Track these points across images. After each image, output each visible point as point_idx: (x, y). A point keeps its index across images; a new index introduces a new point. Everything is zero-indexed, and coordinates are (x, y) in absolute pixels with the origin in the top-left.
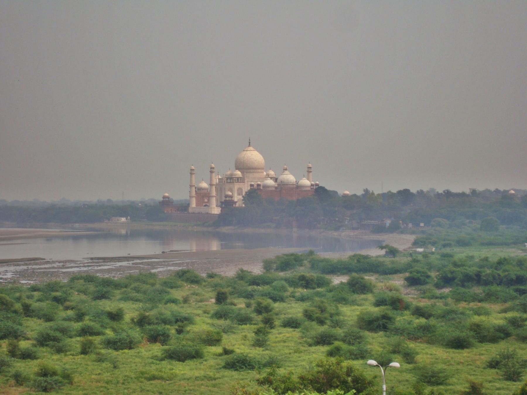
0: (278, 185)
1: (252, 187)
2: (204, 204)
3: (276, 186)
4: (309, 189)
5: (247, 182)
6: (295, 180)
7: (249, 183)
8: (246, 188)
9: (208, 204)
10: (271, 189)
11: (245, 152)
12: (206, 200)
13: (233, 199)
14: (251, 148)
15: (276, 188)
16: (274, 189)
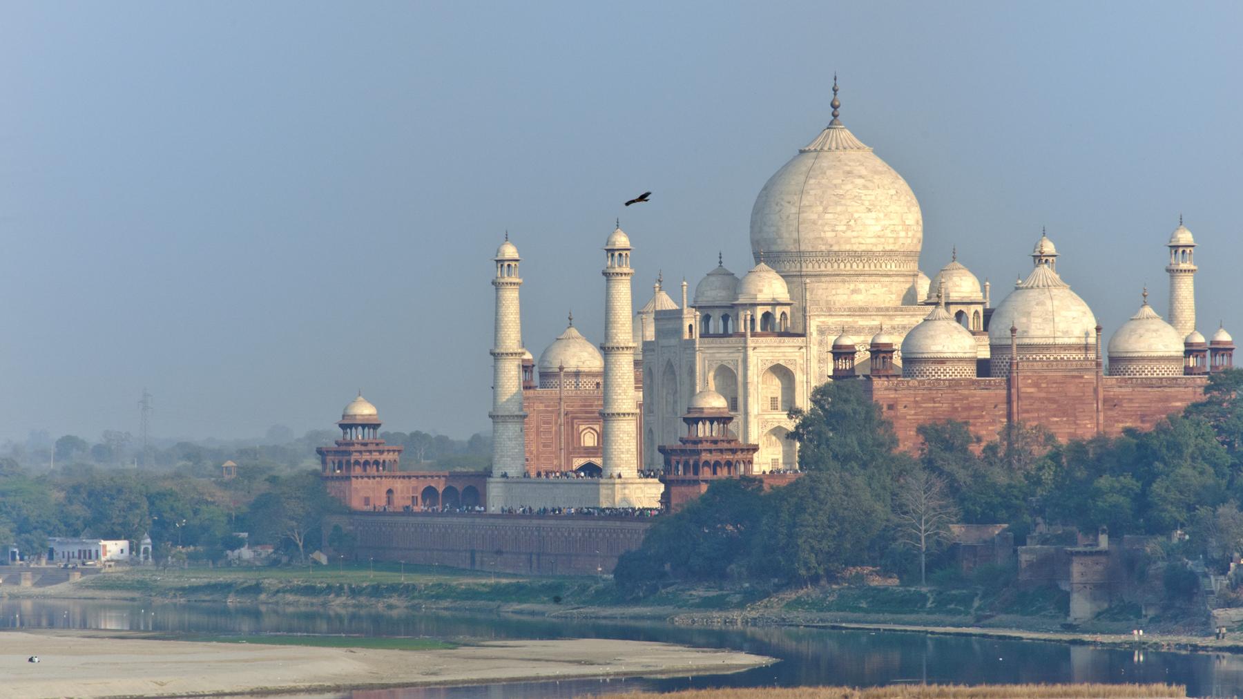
0: (993, 348)
1: (844, 365)
2: (579, 462)
3: (985, 354)
4: (1175, 371)
5: (821, 332)
6: (1090, 323)
7: (831, 339)
8: (814, 365)
9: (598, 461)
10: (949, 372)
11: (808, 161)
12: (589, 440)
13: (731, 426)
14: (844, 135)
15: (983, 367)
16: (970, 372)
